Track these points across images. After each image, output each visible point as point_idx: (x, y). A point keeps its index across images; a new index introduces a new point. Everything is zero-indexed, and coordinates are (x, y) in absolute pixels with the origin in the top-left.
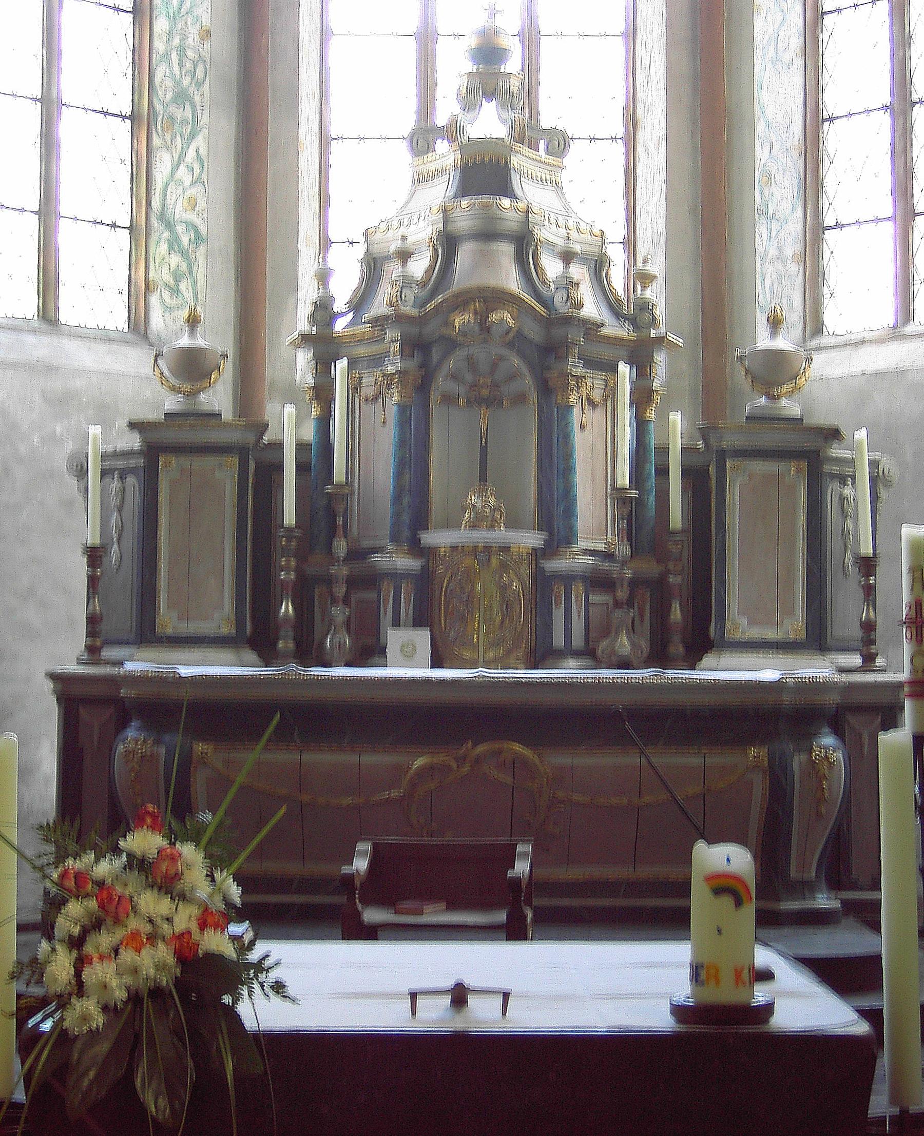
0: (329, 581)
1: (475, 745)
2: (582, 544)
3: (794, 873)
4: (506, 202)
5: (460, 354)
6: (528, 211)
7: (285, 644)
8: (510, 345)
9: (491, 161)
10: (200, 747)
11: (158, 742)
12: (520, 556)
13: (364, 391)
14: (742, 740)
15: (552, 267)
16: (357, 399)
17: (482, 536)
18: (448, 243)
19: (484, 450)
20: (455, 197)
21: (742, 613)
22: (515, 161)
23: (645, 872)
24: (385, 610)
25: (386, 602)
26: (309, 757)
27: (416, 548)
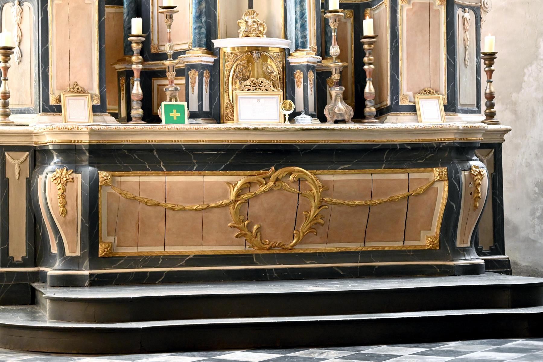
1: (276, 170)
3: (458, 245)
7: (137, 111)
10: (103, 174)
11: (76, 171)
14: (430, 164)
17: (253, 42)
21: (408, 90)
23: (371, 246)
24: (193, 89)
25: (193, 83)
26: (170, 179)
27: (210, 50)
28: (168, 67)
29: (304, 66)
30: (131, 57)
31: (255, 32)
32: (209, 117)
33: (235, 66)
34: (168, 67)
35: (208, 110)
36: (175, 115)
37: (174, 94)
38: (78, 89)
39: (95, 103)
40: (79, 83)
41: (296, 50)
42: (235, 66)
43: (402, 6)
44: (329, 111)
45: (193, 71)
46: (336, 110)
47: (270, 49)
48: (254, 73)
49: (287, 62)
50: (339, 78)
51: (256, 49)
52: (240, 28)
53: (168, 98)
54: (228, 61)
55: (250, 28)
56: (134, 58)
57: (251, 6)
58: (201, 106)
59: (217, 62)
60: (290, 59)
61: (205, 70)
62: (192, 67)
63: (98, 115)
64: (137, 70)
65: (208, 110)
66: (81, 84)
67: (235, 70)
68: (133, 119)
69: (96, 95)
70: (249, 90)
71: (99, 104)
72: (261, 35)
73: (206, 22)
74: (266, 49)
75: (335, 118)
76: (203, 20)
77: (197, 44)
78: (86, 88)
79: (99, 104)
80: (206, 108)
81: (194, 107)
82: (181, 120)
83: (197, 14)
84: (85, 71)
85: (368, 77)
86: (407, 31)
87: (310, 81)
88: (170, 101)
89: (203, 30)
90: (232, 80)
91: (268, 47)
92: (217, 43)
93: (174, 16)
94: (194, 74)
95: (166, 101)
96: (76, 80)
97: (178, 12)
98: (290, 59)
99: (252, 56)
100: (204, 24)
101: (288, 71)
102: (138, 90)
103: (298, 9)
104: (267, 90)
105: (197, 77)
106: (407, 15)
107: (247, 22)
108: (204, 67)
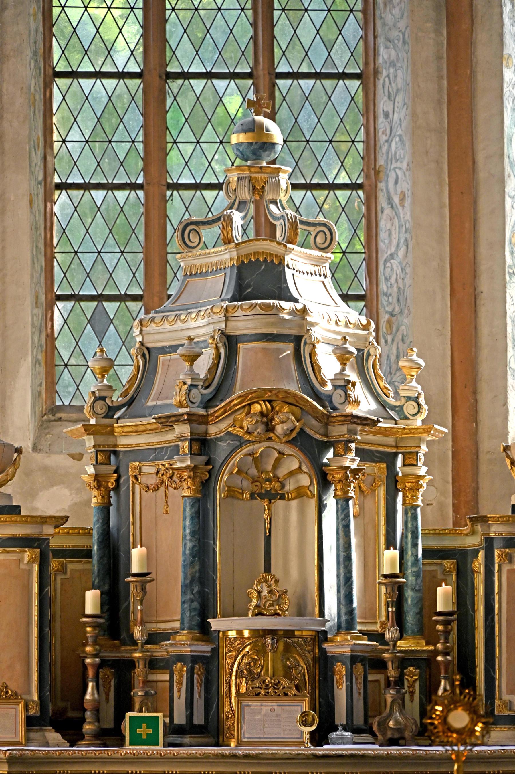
0: (131, 664)
2: (359, 627)
4: (286, 305)
5: (246, 450)
6: (304, 311)
8: (292, 442)
9: (265, 260)
12: (305, 639)
13: (144, 480)
15: (329, 366)
16: (137, 487)
18: (231, 342)
19: (268, 540)
20: (233, 299)
22: (288, 259)
24: (179, 691)
25: (180, 683)
28: (138, 660)
29: (346, 657)
30: (84, 649)
31: (272, 608)
32: (203, 733)
33: (240, 657)
34: (138, 660)
35: (202, 723)
36: (144, 731)
37: (146, 701)
38: (7, 693)
39: (31, 712)
40: (8, 684)
41: (338, 634)
42: (240, 657)
43: (500, 566)
44: (379, 725)
45: (179, 665)
46: (391, 724)
47: (296, 633)
48: (267, 670)
49: (323, 651)
50: (397, 675)
51: (272, 632)
52: (251, 601)
53: (137, 706)
54: (230, 651)
55: (264, 601)
56: (88, 649)
57: (268, 569)
58: (190, 716)
59: (216, 651)
60: (325, 645)
61: (197, 663)
62: (180, 658)
63: (37, 731)
64: (92, 665)
65: (202, 723)
66: (13, 686)
67: (240, 663)
68: (87, 737)
69: (33, 701)
70: (258, 694)
71: (38, 714)
72: (280, 612)
73: (199, 592)
74: (289, 633)
75: (389, 735)
76: (196, 590)
77: (187, 625)
78: (19, 692)
79: (38, 714)
80: (199, 720)
81: (180, 718)
82: (153, 741)
83: (188, 581)
84: (19, 667)
85: (442, 675)
86: (508, 603)
87: (357, 679)
88: (140, 711)
89: (196, 605)
90: (236, 679)
91: (293, 631)
92: (215, 624)
93: (148, 586)
94: (181, 670)
95: (133, 711)
96: (4, 681)
97: (153, 580)
98: (325, 645)
99: (264, 645)
100: (197, 596)
101: (325, 663)
102: (93, 694)
103: (342, 571)
104: (286, 695)
105: (185, 674)
106: (508, 578)
107: (259, 593)
108: (195, 659)
